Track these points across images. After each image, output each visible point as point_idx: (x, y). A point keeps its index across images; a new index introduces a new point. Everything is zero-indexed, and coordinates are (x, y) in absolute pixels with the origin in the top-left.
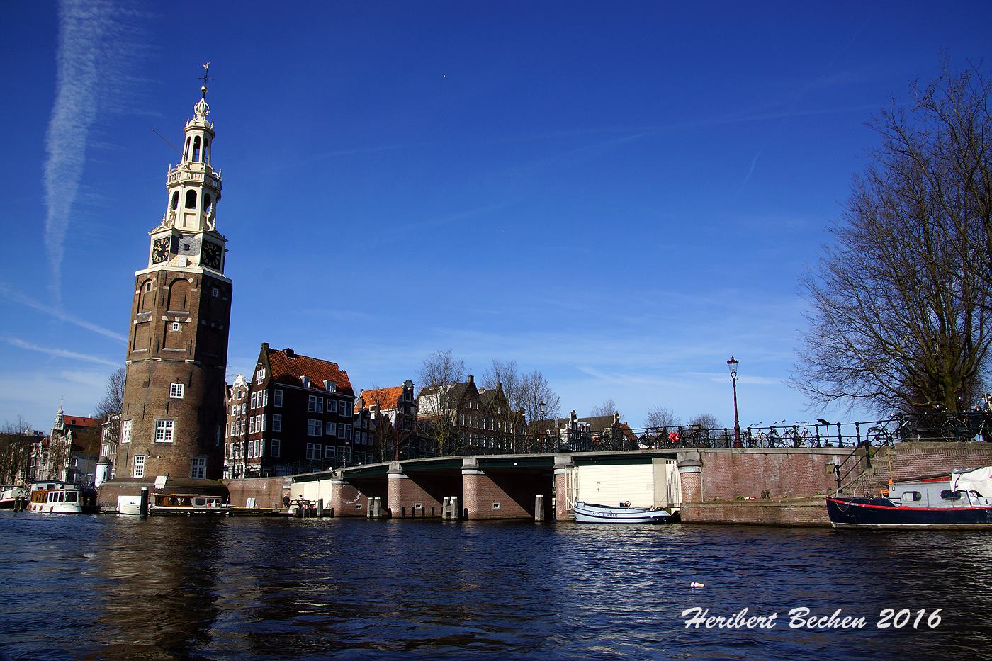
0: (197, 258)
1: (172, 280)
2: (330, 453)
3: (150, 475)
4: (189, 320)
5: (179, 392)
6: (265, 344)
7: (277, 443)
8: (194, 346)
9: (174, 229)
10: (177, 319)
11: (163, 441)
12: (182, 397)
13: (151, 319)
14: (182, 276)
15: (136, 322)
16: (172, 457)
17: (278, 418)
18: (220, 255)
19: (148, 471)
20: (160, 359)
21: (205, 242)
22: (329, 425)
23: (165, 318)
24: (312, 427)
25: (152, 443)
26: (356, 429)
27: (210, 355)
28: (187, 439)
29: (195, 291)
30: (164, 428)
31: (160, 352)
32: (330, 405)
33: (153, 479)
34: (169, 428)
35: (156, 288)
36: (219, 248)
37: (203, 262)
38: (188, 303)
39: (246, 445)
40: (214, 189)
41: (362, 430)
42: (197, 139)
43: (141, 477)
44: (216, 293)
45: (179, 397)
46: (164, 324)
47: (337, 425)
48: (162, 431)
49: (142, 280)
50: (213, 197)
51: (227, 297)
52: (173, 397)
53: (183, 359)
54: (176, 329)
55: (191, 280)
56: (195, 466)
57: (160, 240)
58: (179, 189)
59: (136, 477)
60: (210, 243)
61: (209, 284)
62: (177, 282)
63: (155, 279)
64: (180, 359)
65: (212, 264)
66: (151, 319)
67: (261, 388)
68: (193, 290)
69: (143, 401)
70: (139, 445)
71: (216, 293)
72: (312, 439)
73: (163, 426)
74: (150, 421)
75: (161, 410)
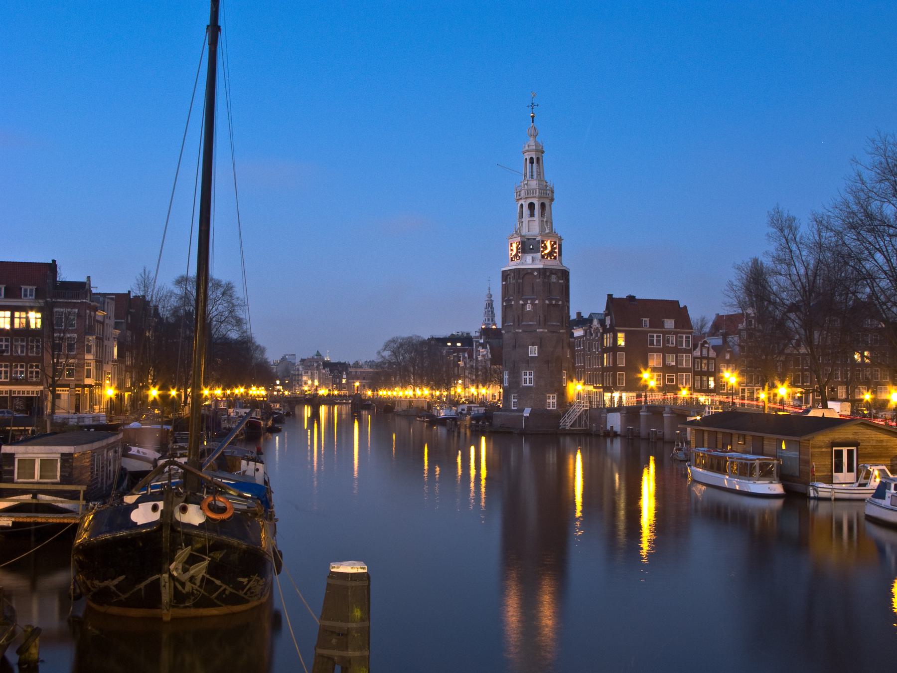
2: (671, 380)
4: (537, 302)
9: (522, 236)
23: (521, 302)
26: (695, 358)
30: (528, 377)
32: (668, 340)
33: (522, 411)
39: (602, 374)
42: (532, 159)
44: (554, 279)
50: (547, 202)
54: (529, 307)
55: (536, 274)
58: (522, 202)
61: (548, 274)
71: (554, 279)
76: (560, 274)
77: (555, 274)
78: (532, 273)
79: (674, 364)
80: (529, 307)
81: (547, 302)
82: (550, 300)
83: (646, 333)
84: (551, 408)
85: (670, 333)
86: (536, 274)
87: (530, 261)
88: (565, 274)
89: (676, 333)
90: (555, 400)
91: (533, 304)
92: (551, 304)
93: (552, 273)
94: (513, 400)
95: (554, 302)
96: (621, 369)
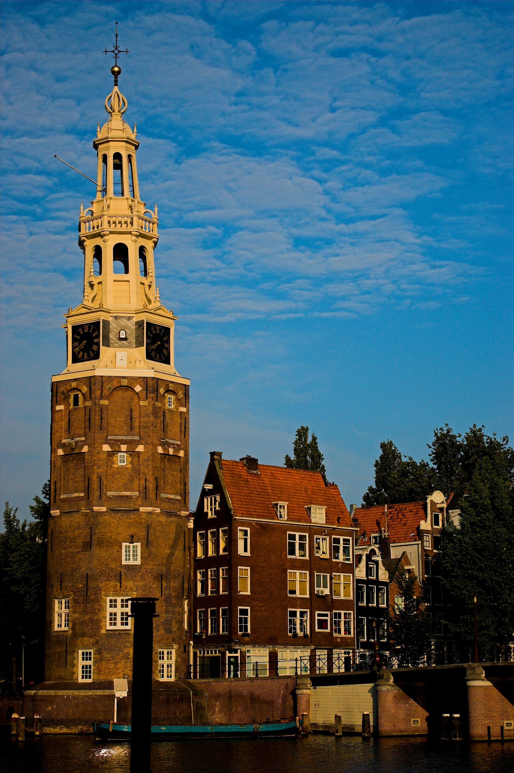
2: (322, 624)
3: (102, 678)
6: (212, 454)
10: (124, 448)
11: (119, 627)
12: (138, 562)
13: (85, 449)
14: (125, 382)
19: (99, 671)
20: (104, 509)
23: (106, 448)
24: (298, 582)
25: (103, 631)
26: (359, 581)
27: (172, 497)
31: (104, 497)
35: (88, 404)
41: (368, 582)
42: (118, 156)
43: (90, 681)
45: (135, 563)
46: (105, 456)
47: (331, 578)
48: (115, 614)
51: (185, 406)
52: (128, 563)
53: (136, 507)
54: (122, 460)
55: (138, 388)
56: (160, 662)
57: (82, 326)
59: (80, 680)
61: (162, 391)
62: (119, 395)
63: (85, 389)
64: (132, 506)
65: (160, 357)
66: (85, 449)
67: (215, 524)
68: (142, 403)
70: (83, 635)
72: (295, 603)
73: (115, 606)
74: (98, 600)
75: (112, 583)
76: (181, 395)
77: (174, 393)
79: (327, 591)
80: (122, 460)
81: (160, 450)
83: (283, 529)
84: (165, 679)
85: (320, 530)
86: (138, 388)
87: (125, 363)
89: (331, 532)
90: (173, 662)
91: (131, 452)
92: (166, 455)
93: (168, 391)
94: (81, 663)
95: (171, 451)
96: (244, 600)
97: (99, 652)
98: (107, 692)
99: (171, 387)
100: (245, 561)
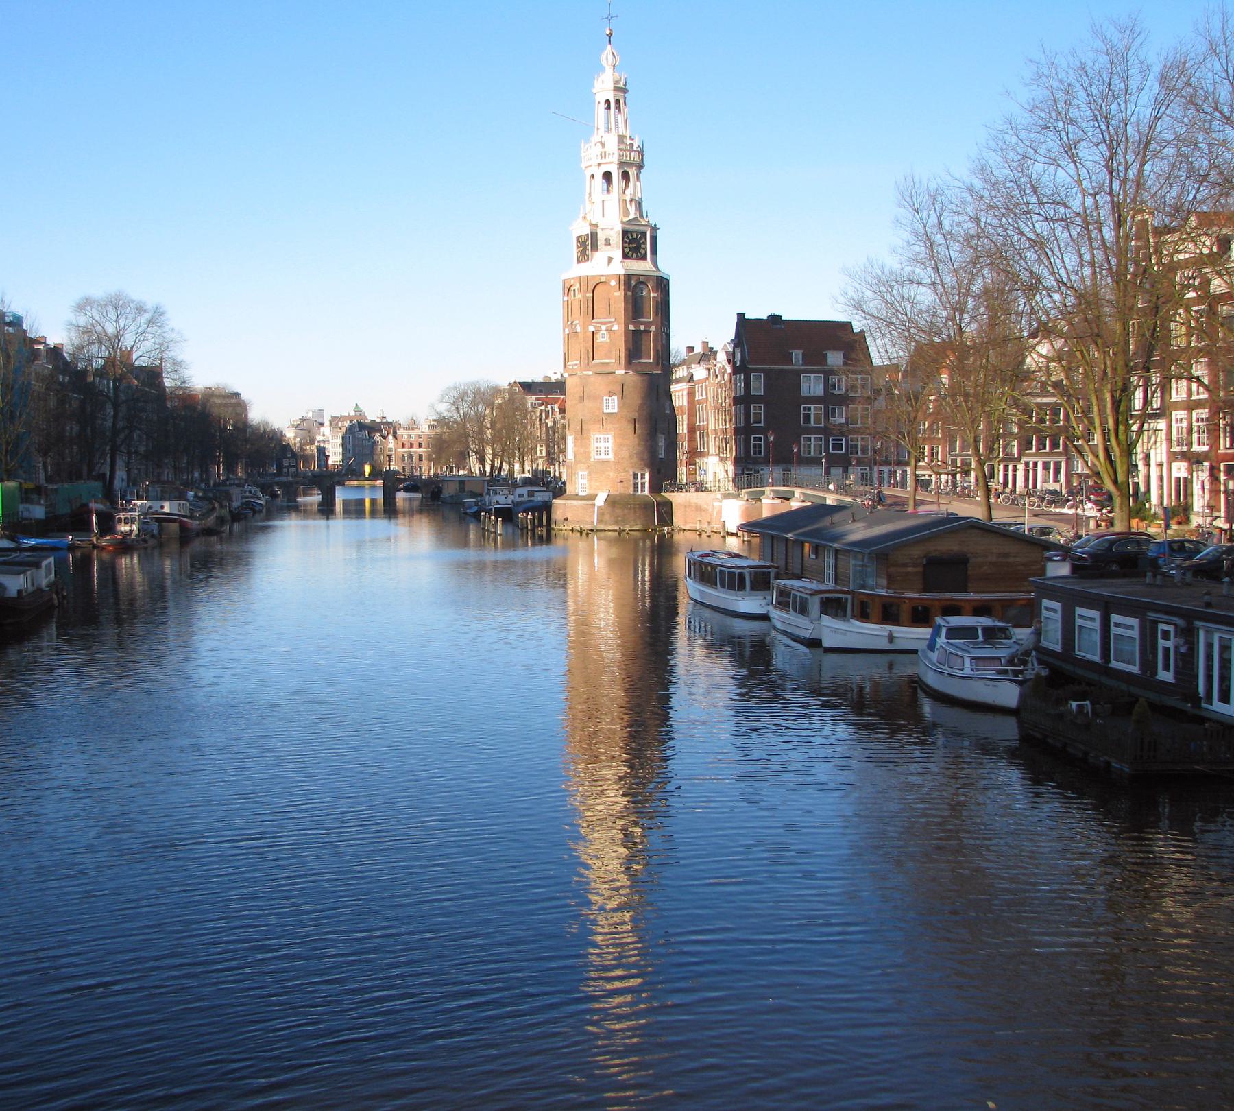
0: (618, 254)
1: (594, 285)
3: (593, 492)
5: (612, 405)
6: (739, 315)
7: (760, 439)
8: (623, 355)
10: (604, 327)
12: (616, 411)
14: (603, 279)
15: (567, 332)
16: (612, 474)
17: (758, 409)
18: (645, 243)
19: (591, 488)
21: (625, 233)
22: (834, 410)
23: (591, 328)
28: (625, 453)
29: (619, 295)
34: (607, 445)
36: (644, 234)
37: (625, 256)
38: (612, 309)
40: (631, 164)
42: (608, 102)
49: (567, 286)
60: (631, 232)
61: (633, 283)
63: (578, 286)
69: (580, 417)
70: (580, 462)
74: (588, 438)
78: (606, 283)
79: (842, 421)
82: (637, 324)
83: (798, 373)
86: (613, 283)
88: (662, 284)
91: (609, 330)
95: (642, 328)
97: (590, 474)
98: (590, 502)
99: (642, 279)
100: (758, 399)
